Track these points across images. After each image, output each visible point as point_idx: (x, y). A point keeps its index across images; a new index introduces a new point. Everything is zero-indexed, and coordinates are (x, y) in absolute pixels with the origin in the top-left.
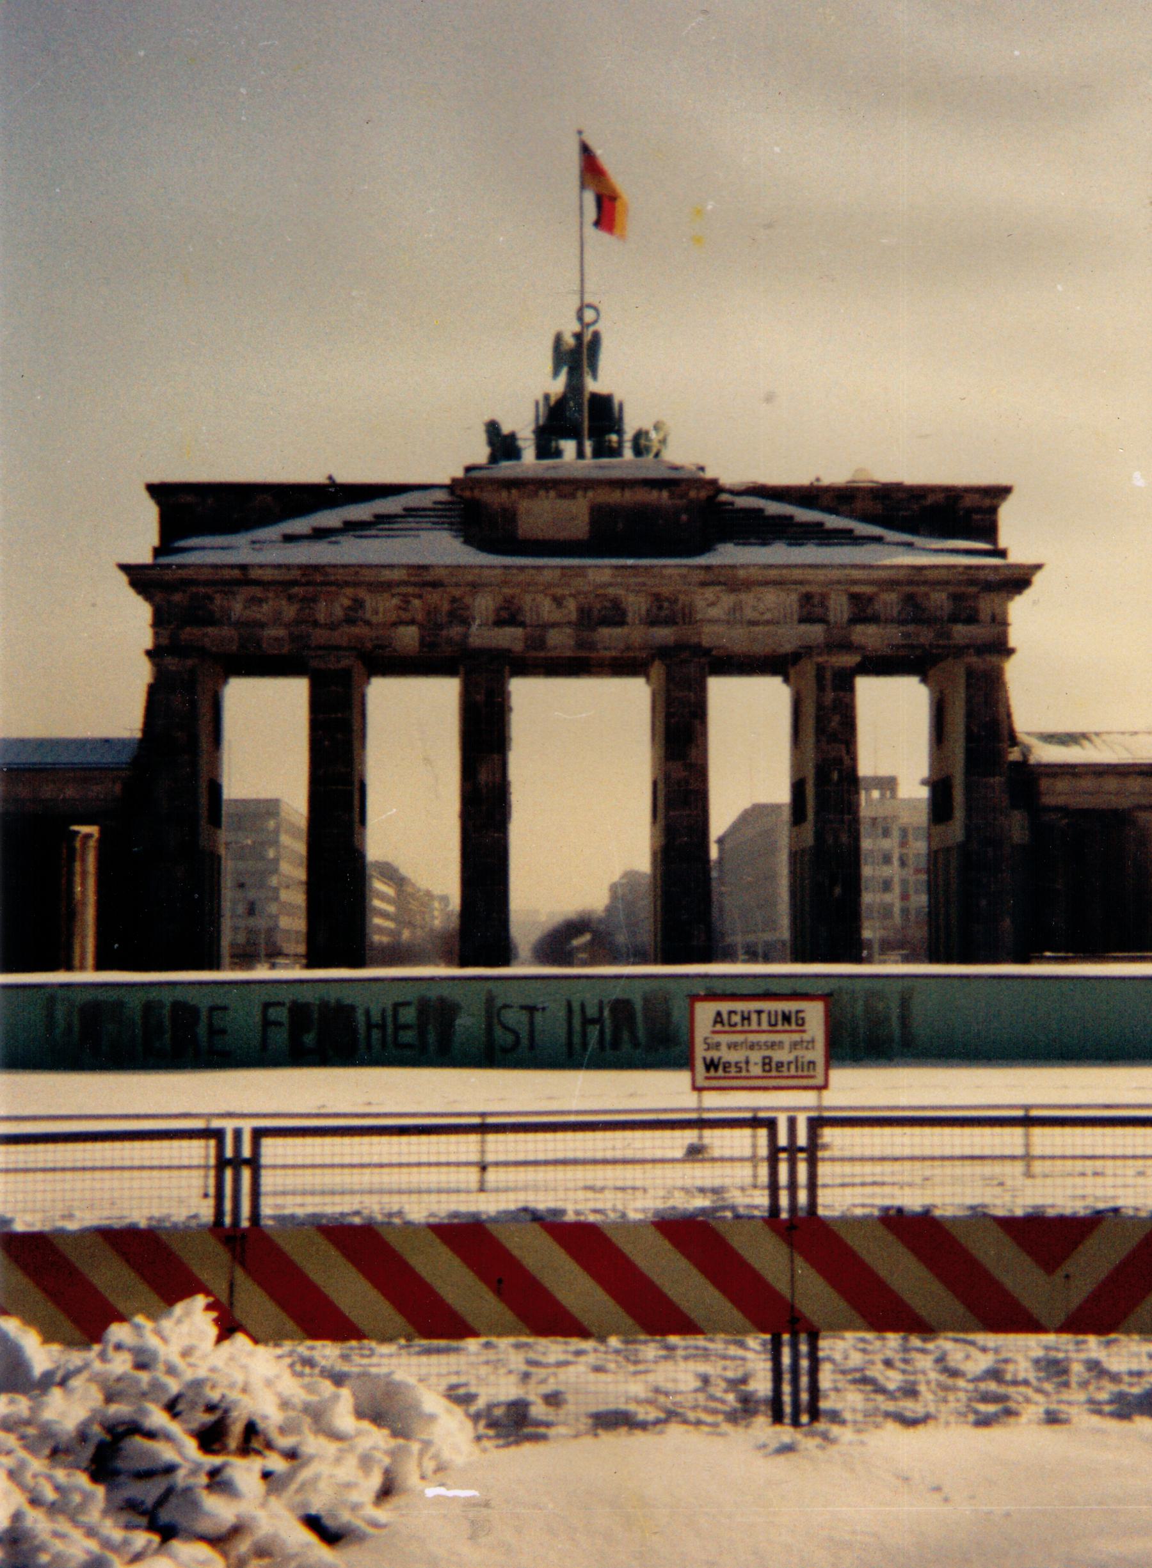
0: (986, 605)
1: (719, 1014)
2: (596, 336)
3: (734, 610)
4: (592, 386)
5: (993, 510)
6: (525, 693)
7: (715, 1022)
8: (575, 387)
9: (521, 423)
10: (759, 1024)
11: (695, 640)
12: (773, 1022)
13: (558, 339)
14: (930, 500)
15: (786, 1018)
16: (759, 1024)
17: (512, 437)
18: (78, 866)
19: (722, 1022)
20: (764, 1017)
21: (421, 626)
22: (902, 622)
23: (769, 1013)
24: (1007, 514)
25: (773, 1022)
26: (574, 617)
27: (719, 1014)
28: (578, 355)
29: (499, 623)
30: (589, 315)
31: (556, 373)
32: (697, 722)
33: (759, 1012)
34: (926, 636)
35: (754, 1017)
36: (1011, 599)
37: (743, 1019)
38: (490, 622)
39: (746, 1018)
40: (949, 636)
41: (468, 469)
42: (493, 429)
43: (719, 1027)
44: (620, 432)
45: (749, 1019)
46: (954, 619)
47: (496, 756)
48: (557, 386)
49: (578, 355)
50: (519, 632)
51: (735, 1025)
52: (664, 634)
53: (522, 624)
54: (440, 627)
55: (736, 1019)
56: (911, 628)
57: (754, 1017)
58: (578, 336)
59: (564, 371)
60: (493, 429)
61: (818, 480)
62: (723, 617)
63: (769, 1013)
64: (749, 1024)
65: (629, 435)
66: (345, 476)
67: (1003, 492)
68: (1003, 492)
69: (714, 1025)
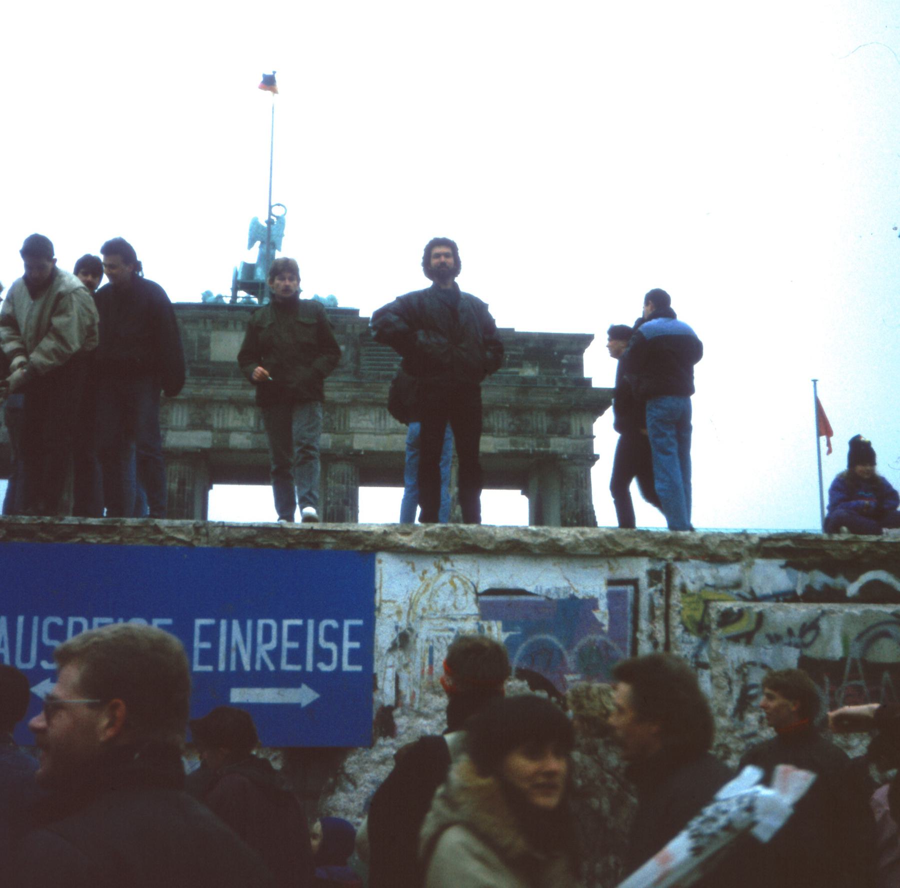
0: (575, 424)
3: (380, 419)
4: (279, 255)
5: (580, 352)
8: (266, 256)
11: (347, 442)
13: (255, 223)
14: (531, 345)
22: (513, 433)
26: (252, 423)
28: (267, 235)
29: (193, 426)
32: (347, 508)
34: (528, 444)
36: (594, 421)
38: (185, 424)
46: (552, 431)
48: (253, 256)
50: (208, 434)
53: (209, 428)
56: (520, 439)
59: (258, 243)
62: (371, 426)
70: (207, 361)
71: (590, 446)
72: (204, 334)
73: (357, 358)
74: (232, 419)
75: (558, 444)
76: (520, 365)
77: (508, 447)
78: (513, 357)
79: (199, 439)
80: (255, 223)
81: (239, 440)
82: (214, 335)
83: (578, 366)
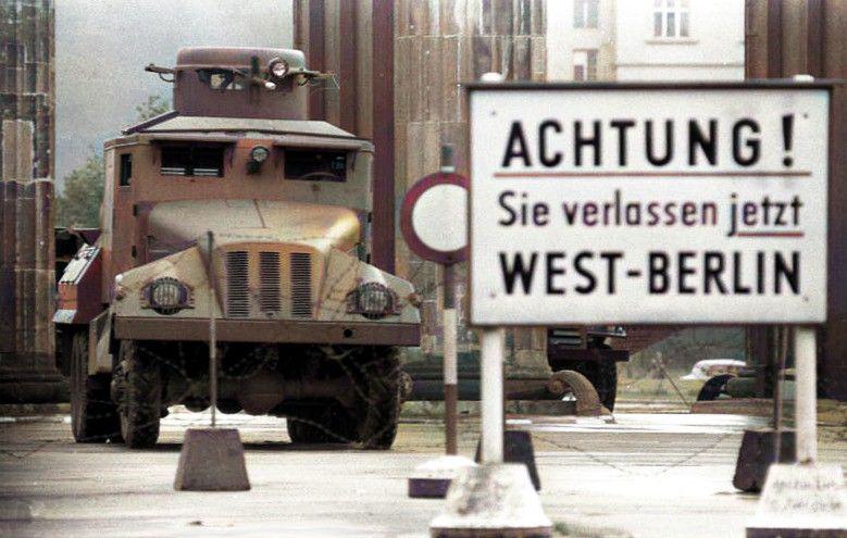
1: (517, 131)
7: (509, 156)
10: (622, 161)
12: (659, 152)
15: (702, 141)
16: (622, 161)
18: (19, 55)
19: (524, 155)
20: (635, 137)
23: (649, 125)
25: (659, 152)
27: (517, 131)
33: (622, 126)
35: (610, 137)
37: (580, 143)
39: (587, 142)
43: (517, 164)
45: (596, 142)
51: (558, 159)
55: (560, 143)
57: (610, 137)
63: (649, 125)
64: (597, 161)
69: (506, 163)
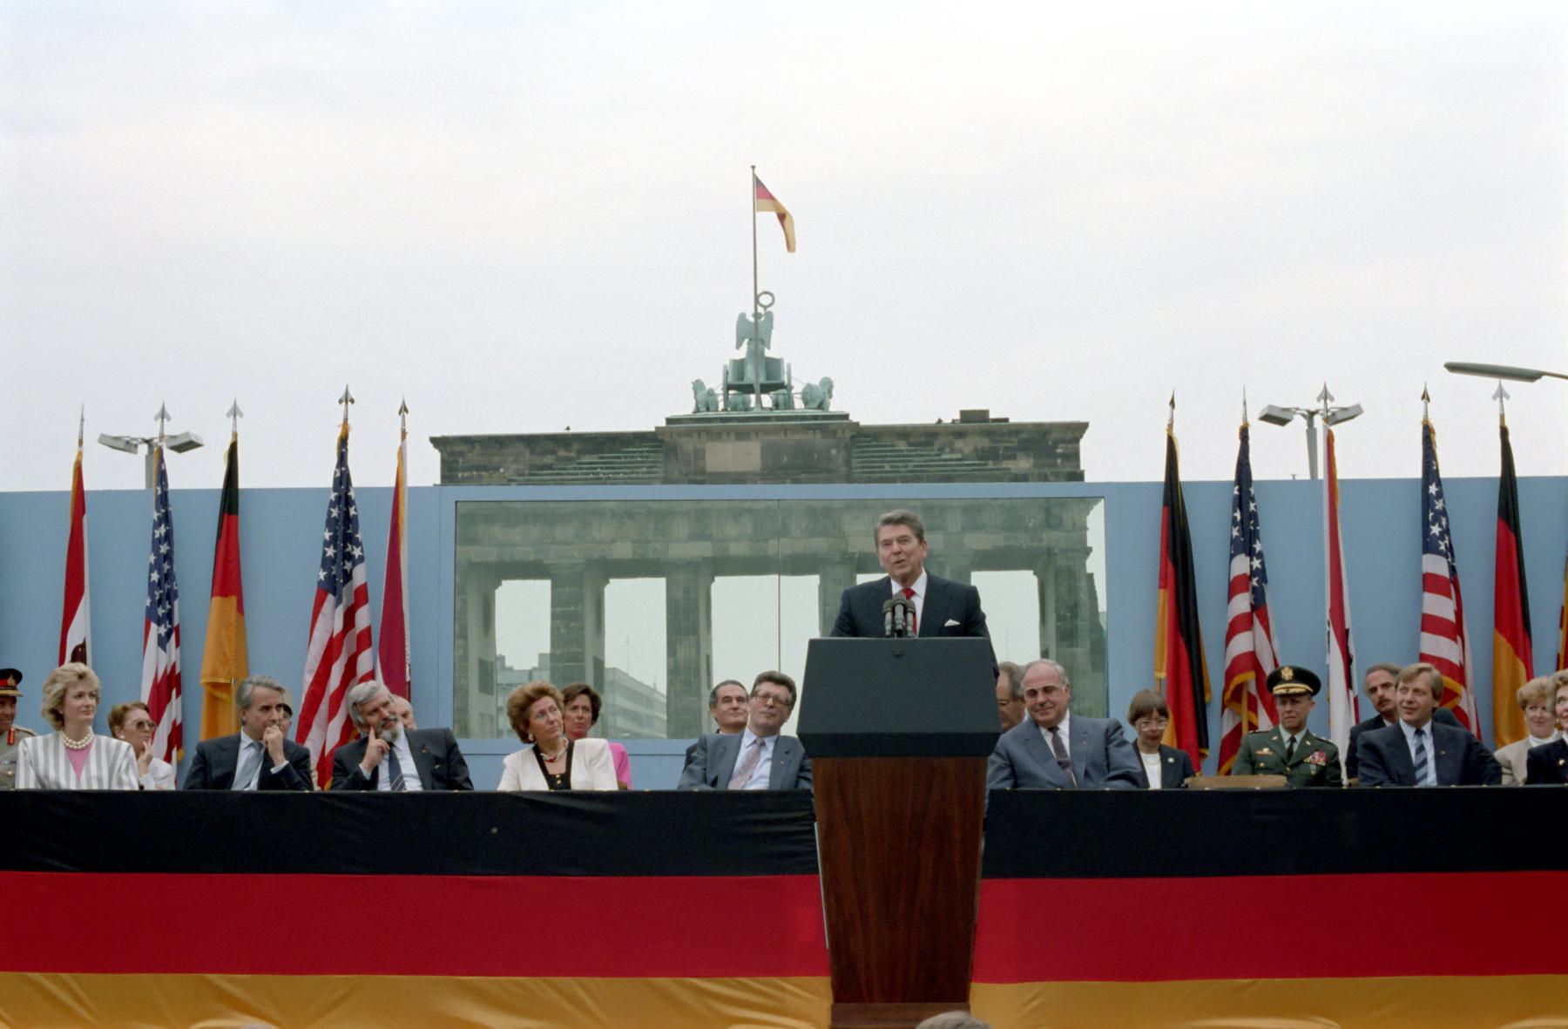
2: (770, 316)
4: (768, 353)
5: (1077, 440)
6: (726, 591)
8: (756, 353)
9: (715, 383)
13: (742, 317)
14: (1024, 436)
17: (711, 393)
21: (634, 541)
24: (1086, 444)
28: (755, 331)
30: (765, 300)
31: (739, 346)
40: (1040, 540)
41: (669, 421)
42: (698, 386)
44: (789, 387)
47: (692, 638)
48: (742, 354)
49: (755, 331)
52: (819, 545)
53: (708, 537)
54: (649, 542)
58: (757, 315)
60: (698, 386)
61: (940, 421)
65: (797, 389)
66: (576, 429)
67: (1082, 428)
68: (1082, 428)
70: (703, 472)
71: (1083, 539)
72: (699, 446)
73: (848, 463)
74: (730, 530)
75: (1050, 538)
76: (1014, 457)
77: (1002, 543)
78: (1007, 448)
79: (700, 550)
80: (742, 317)
81: (738, 549)
82: (709, 446)
83: (1075, 456)
